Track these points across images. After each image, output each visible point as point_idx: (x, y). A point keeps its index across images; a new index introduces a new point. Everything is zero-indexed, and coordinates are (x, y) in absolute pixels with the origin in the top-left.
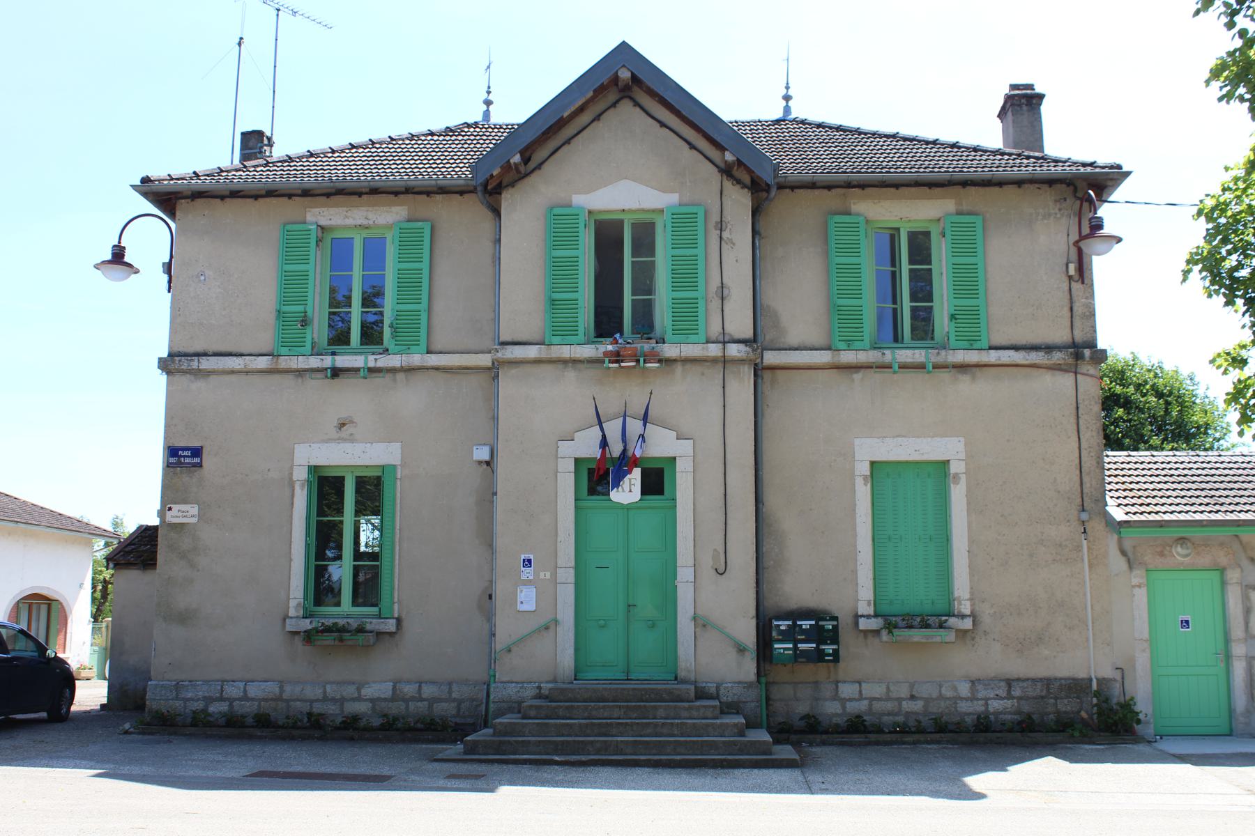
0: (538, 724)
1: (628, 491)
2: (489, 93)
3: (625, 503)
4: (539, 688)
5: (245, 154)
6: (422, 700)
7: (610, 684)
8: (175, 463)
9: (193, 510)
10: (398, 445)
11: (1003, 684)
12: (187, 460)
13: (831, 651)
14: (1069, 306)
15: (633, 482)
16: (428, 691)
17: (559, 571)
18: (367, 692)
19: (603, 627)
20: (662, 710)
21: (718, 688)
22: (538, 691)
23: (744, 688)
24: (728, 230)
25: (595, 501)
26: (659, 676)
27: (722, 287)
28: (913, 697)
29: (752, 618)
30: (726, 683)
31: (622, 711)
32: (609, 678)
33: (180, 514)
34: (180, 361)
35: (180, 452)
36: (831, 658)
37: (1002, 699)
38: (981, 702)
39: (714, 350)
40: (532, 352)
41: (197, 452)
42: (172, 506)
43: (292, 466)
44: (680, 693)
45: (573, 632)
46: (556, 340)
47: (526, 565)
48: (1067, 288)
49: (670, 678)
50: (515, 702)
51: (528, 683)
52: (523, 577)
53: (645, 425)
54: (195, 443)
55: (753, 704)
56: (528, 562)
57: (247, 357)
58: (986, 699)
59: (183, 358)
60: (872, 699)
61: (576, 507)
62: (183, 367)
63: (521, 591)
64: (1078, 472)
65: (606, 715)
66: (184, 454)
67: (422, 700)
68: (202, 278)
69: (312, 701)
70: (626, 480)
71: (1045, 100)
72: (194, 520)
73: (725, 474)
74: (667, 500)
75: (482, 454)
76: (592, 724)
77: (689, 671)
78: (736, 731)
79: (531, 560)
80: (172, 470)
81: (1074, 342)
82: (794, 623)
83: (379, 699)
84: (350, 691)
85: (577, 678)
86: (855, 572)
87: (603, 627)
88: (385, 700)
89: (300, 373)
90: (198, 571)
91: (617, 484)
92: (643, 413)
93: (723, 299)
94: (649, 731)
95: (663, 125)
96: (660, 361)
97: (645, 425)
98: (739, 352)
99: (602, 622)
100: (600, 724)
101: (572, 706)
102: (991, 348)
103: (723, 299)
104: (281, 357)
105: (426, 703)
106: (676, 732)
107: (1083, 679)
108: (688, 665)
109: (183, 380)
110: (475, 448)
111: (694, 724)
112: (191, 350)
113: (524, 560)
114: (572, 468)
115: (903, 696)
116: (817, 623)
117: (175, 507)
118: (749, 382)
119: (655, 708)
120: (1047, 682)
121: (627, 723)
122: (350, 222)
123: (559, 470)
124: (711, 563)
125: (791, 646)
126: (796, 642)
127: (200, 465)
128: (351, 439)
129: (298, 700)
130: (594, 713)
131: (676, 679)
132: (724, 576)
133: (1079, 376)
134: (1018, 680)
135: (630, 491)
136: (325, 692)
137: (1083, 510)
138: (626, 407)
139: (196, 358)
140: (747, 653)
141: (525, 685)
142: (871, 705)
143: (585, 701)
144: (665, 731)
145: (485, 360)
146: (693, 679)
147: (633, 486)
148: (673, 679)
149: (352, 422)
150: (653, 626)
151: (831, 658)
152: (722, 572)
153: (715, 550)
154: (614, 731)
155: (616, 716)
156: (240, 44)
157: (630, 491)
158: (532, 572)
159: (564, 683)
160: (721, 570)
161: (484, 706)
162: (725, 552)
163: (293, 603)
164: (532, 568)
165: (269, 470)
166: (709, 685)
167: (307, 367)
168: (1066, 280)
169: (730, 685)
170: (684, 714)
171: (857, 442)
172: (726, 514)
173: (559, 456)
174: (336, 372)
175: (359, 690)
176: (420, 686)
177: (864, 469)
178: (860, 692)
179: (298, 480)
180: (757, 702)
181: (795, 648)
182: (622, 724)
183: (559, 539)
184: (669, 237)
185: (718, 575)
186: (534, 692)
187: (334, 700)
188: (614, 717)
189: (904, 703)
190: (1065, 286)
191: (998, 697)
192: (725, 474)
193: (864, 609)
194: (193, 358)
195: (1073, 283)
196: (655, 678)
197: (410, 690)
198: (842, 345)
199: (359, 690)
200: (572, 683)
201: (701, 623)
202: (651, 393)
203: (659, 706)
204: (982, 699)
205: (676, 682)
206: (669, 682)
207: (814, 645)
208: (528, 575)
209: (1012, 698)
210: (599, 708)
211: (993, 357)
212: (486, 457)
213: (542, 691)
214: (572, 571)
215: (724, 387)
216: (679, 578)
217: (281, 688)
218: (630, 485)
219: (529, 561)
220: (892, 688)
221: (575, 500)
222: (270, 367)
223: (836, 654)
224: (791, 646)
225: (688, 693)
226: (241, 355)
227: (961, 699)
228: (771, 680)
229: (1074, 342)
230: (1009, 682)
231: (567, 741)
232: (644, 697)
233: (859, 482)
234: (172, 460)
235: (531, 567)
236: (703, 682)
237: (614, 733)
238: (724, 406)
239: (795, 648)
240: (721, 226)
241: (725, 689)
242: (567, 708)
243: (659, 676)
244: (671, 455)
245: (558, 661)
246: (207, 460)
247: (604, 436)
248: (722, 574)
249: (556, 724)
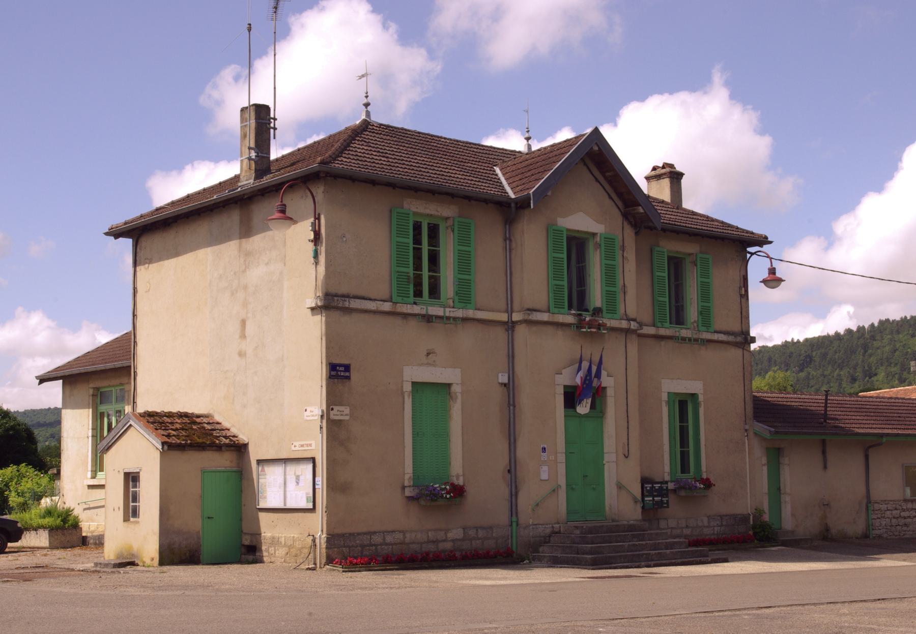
1: (583, 408)
2: (367, 97)
3: (582, 414)
4: (553, 527)
5: (259, 123)
6: (479, 539)
8: (334, 376)
9: (347, 410)
10: (460, 369)
11: (719, 518)
12: (342, 374)
13: (666, 501)
14: (740, 310)
16: (481, 534)
18: (451, 535)
24: (626, 251)
25: (571, 411)
27: (624, 286)
28: (687, 527)
33: (339, 413)
34: (338, 300)
35: (338, 368)
36: (666, 505)
37: (719, 526)
38: (712, 528)
39: (624, 324)
40: (545, 317)
41: (347, 368)
42: (334, 407)
43: (403, 381)
46: (556, 310)
48: (739, 301)
51: (547, 524)
54: (346, 362)
56: (544, 450)
57: (378, 302)
58: (714, 526)
59: (339, 298)
60: (672, 528)
62: (339, 305)
64: (744, 403)
66: (340, 369)
67: (479, 539)
68: (345, 239)
69: (421, 543)
71: (684, 176)
72: (347, 418)
75: (504, 378)
80: (332, 380)
81: (742, 332)
82: (653, 485)
83: (457, 540)
84: (441, 535)
86: (663, 456)
88: (460, 540)
89: (405, 316)
90: (351, 454)
93: (625, 293)
95: (597, 180)
96: (607, 329)
98: (634, 326)
102: (716, 332)
103: (625, 293)
104: (398, 304)
105: (480, 541)
107: (746, 514)
109: (336, 315)
110: (500, 375)
112: (340, 292)
115: (683, 526)
116: (653, 485)
117: (336, 408)
120: (734, 517)
122: (428, 211)
125: (651, 499)
126: (654, 496)
127: (348, 378)
128: (433, 364)
129: (413, 543)
133: (745, 351)
134: (724, 516)
136: (428, 536)
137: (746, 424)
139: (348, 299)
142: (672, 531)
145: (504, 317)
149: (434, 353)
151: (666, 505)
156: (249, 30)
157: (586, 407)
160: (626, 456)
161: (510, 541)
163: (407, 477)
164: (546, 453)
165: (389, 383)
167: (412, 312)
168: (739, 296)
171: (663, 381)
174: (428, 319)
175: (446, 534)
176: (477, 530)
177: (665, 397)
178: (668, 524)
179: (406, 392)
181: (653, 499)
184: (699, 273)
187: (433, 542)
189: (684, 530)
190: (739, 298)
191: (718, 526)
193: (667, 478)
194: (346, 299)
195: (742, 299)
197: (472, 533)
198: (659, 324)
199: (446, 534)
200: (567, 524)
201: (620, 487)
202: (603, 349)
204: (712, 527)
207: (660, 498)
209: (722, 525)
211: (716, 337)
212: (506, 381)
213: (555, 529)
214: (564, 455)
217: (404, 535)
220: (679, 522)
222: (391, 310)
223: (667, 501)
224: (651, 499)
226: (375, 300)
227: (705, 527)
229: (742, 332)
230: (721, 517)
233: (664, 404)
234: (333, 373)
239: (653, 499)
240: (623, 248)
246: (354, 375)
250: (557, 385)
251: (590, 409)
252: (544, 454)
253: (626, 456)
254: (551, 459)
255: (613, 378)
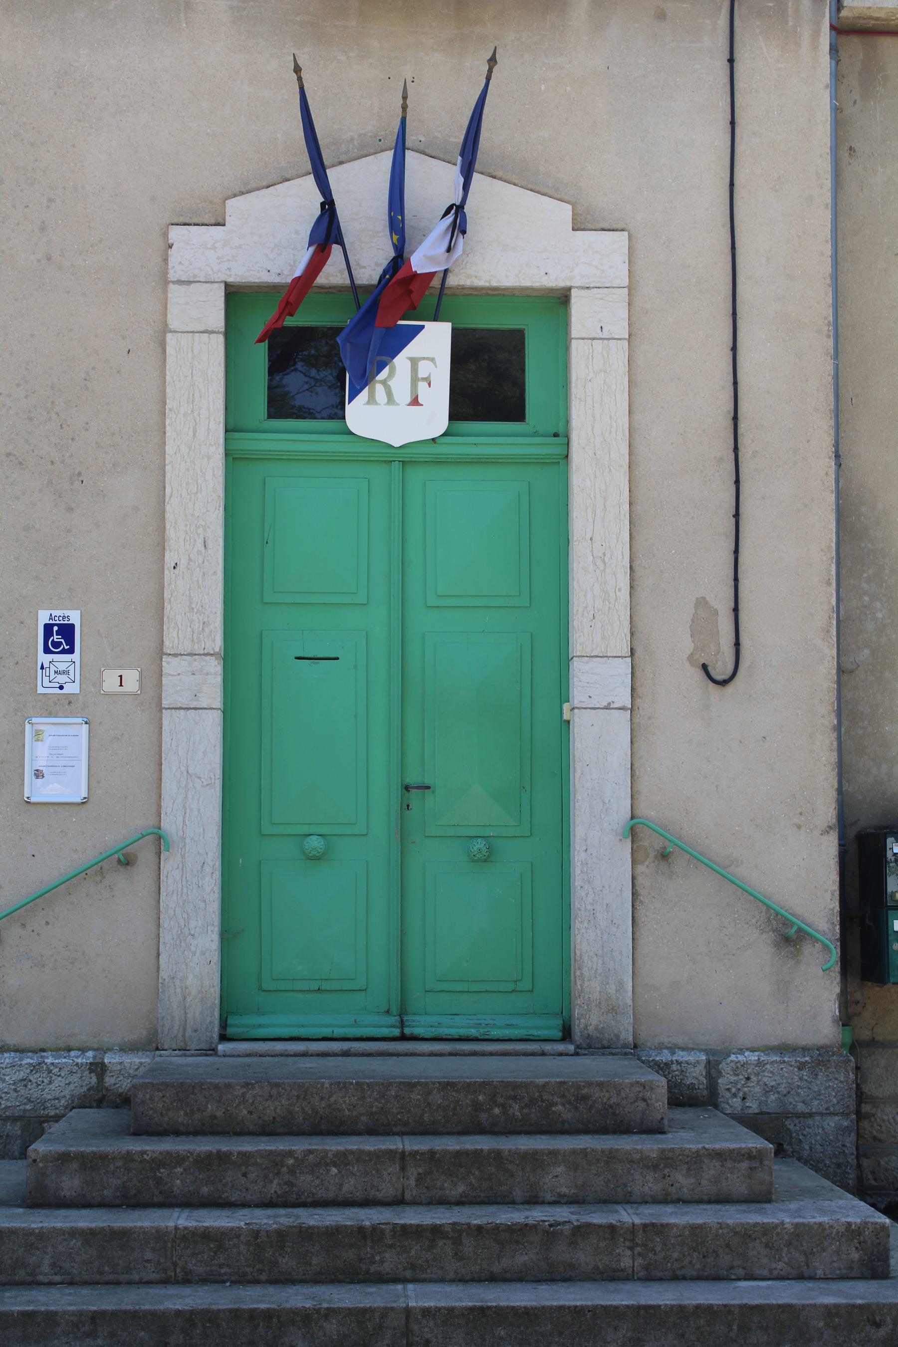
0: (92, 1233)
3: (397, 444)
4: (99, 1068)
7: (346, 1054)
15: (424, 369)
17: (170, 666)
19: (316, 858)
20: (560, 1170)
21: (712, 1068)
22: (94, 1080)
23: (801, 1066)
26: (509, 1026)
29: (826, 832)
30: (741, 1051)
31: (413, 1172)
32: (338, 1032)
44: (614, 1100)
45: (218, 875)
47: (56, 645)
49: (545, 1033)
50: (14, 1119)
52: (45, 686)
53: (467, 173)
55: (831, 1123)
61: (227, 453)
63: (38, 736)
65: (351, 1186)
70: (401, 361)
73: (734, 349)
74: (536, 434)
76: (306, 1234)
77: (613, 1010)
78: (856, 1256)
79: (72, 626)
85: (230, 1031)
87: (316, 858)
91: (364, 380)
92: (465, 121)
94: (523, 1258)
97: (467, 173)
99: (315, 843)
100: (333, 1234)
101: (222, 1158)
106: (626, 1263)
108: (612, 989)
111: (695, 1229)
113: (48, 628)
114: (216, 317)
118: (815, 47)
119: (534, 1159)
121: (436, 1230)
123: (173, 323)
124: (687, 645)
130: (305, 1181)
131: (567, 1034)
132: (730, 689)
135: (415, 402)
138: (404, 108)
140: (809, 951)
141: (49, 1061)
143: (267, 1130)
144: (584, 1257)
146: (627, 1036)
147: (422, 386)
148: (559, 1035)
150: (487, 858)
152: (725, 677)
153: (702, 602)
154: (390, 1261)
155: (387, 1190)
157: (415, 402)
158: (76, 672)
159: (184, 1050)
160: (721, 670)
162: (736, 610)
164: (76, 656)
166: (682, 1056)
169: (753, 1057)
170: (646, 1183)
172: (737, 482)
173: (172, 276)
180: (845, 1115)
182: (416, 1232)
183: (170, 558)
185: (711, 684)
186: (85, 1081)
188: (380, 1195)
192: (734, 349)
196: (495, 1033)
200: (212, 1051)
202: (493, 61)
203: (553, 1153)
205: (571, 1048)
206: (548, 1047)
208: (62, 679)
210: (324, 1161)
213: (109, 1081)
214: (215, 667)
215: (731, 61)
216: (578, 696)
218: (415, 380)
219: (67, 631)
221: (227, 431)
225: (644, 1100)
228: (865, 1034)
231: (209, 1317)
232: (483, 1116)
235: (71, 651)
236: (660, 1047)
237: (387, 1267)
238: (733, 123)
241: (738, 1069)
242: (204, 1162)
243: (509, 1026)
244: (555, 279)
245: (163, 974)
247: (328, 207)
248: (724, 683)
249: (159, 1235)
250: (180, 282)
251: (454, 416)
252: (61, 660)
253: (721, 670)
254: (110, 681)
255: (626, 233)
